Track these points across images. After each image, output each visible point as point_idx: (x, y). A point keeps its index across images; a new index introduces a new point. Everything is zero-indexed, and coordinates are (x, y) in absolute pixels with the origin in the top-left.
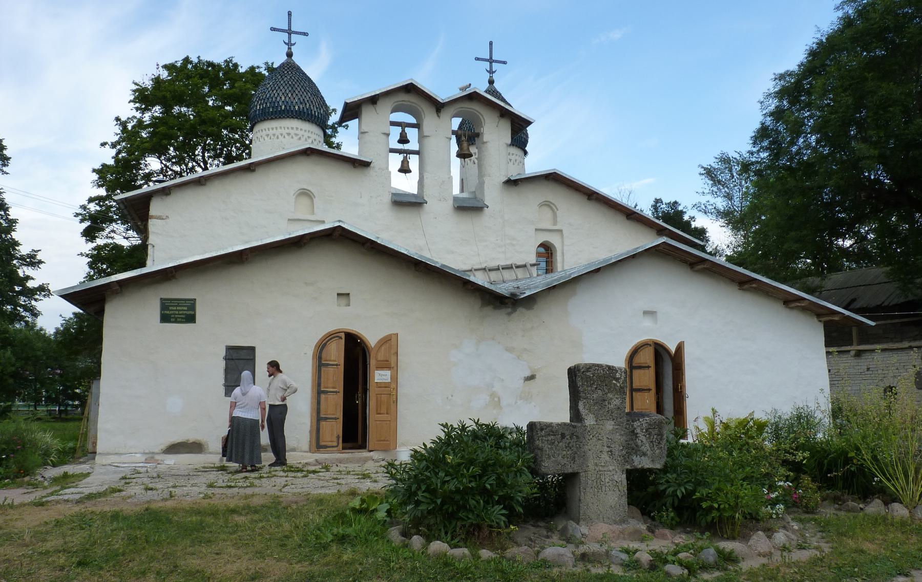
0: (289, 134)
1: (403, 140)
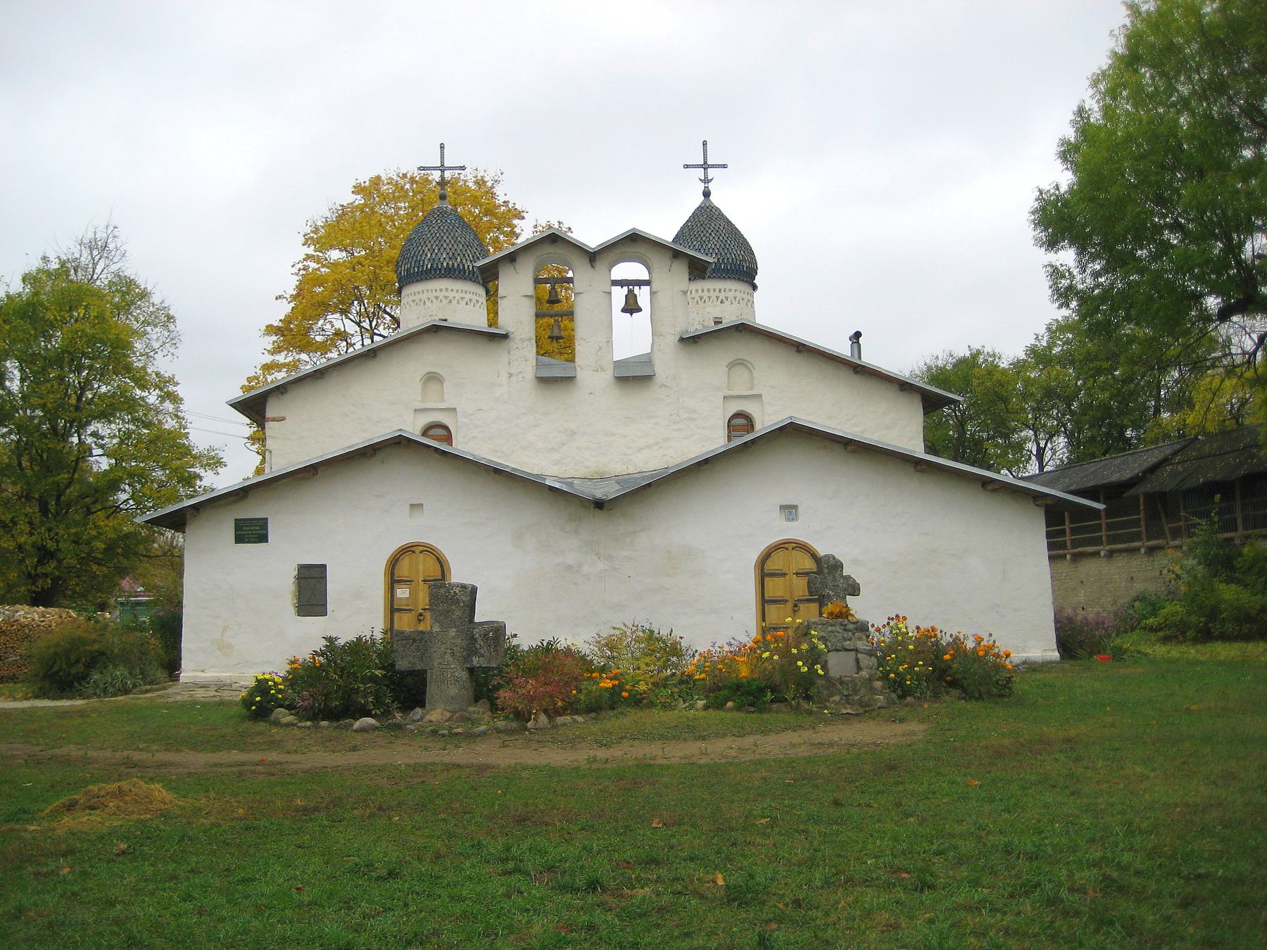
0: (437, 298)
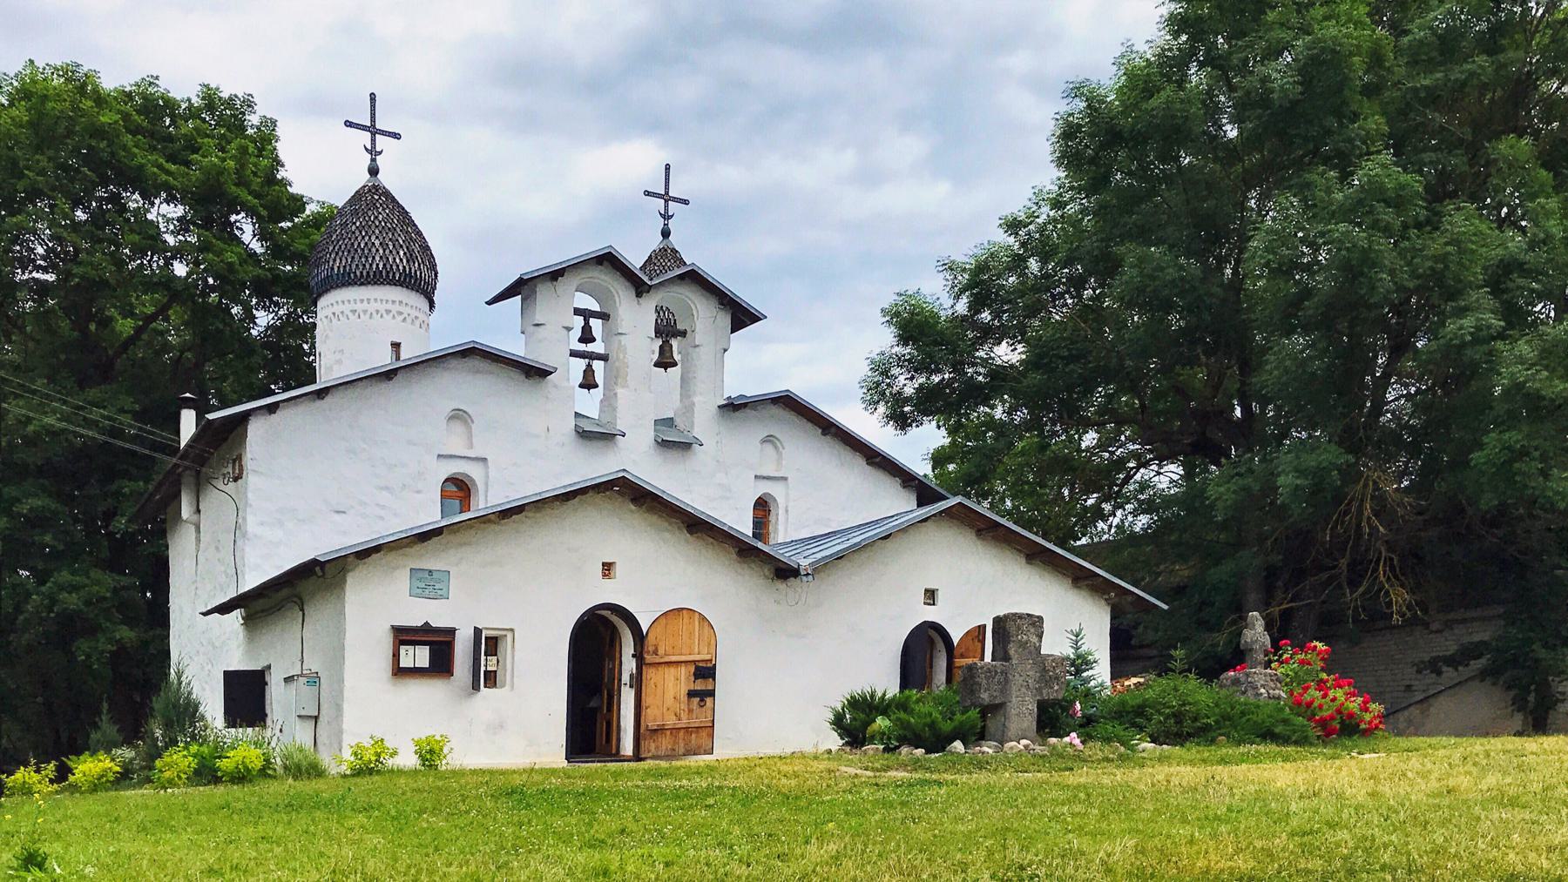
0: (388, 312)
1: (587, 337)
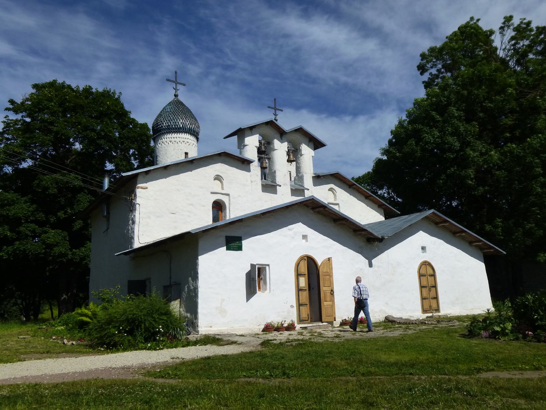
0: (184, 142)
